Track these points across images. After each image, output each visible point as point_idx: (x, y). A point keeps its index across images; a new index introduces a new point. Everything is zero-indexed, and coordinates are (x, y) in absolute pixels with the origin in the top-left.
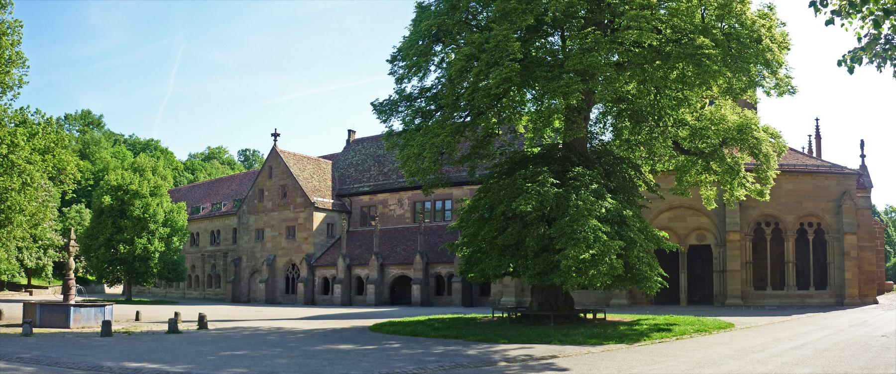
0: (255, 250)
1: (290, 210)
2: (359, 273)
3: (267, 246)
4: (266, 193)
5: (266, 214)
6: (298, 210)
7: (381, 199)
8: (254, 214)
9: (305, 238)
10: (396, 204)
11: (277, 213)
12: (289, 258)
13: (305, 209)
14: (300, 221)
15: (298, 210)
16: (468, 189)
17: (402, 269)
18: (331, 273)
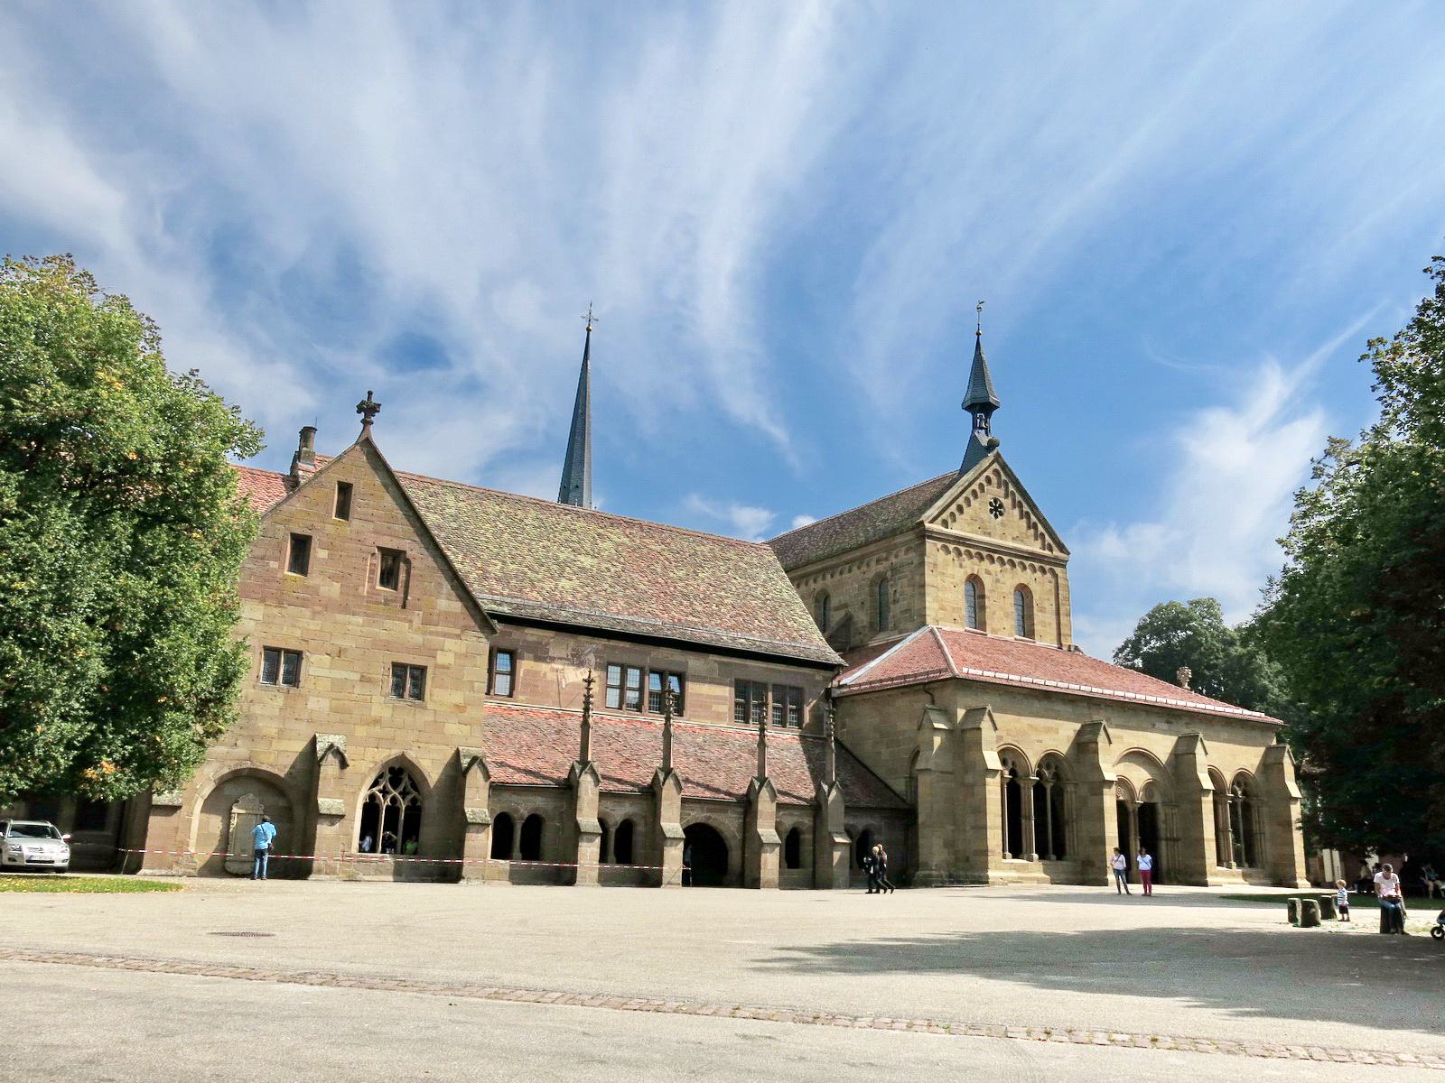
0: (257, 709)
1: (411, 621)
2: (608, 810)
3: (311, 705)
4: (318, 554)
5: (315, 613)
6: (439, 629)
7: (530, 639)
8: (262, 600)
9: (457, 706)
10: (569, 660)
11: (360, 620)
12: (395, 752)
13: (462, 632)
14: (442, 659)
15: (439, 629)
16: (716, 661)
17: (709, 811)
18: (530, 806)
